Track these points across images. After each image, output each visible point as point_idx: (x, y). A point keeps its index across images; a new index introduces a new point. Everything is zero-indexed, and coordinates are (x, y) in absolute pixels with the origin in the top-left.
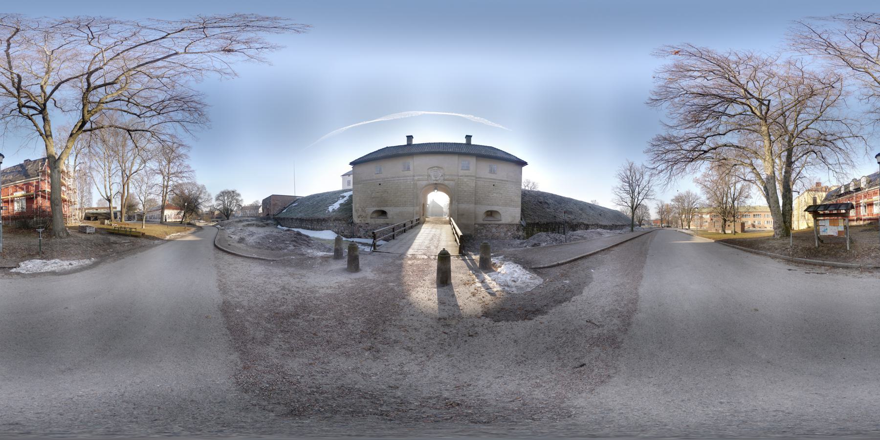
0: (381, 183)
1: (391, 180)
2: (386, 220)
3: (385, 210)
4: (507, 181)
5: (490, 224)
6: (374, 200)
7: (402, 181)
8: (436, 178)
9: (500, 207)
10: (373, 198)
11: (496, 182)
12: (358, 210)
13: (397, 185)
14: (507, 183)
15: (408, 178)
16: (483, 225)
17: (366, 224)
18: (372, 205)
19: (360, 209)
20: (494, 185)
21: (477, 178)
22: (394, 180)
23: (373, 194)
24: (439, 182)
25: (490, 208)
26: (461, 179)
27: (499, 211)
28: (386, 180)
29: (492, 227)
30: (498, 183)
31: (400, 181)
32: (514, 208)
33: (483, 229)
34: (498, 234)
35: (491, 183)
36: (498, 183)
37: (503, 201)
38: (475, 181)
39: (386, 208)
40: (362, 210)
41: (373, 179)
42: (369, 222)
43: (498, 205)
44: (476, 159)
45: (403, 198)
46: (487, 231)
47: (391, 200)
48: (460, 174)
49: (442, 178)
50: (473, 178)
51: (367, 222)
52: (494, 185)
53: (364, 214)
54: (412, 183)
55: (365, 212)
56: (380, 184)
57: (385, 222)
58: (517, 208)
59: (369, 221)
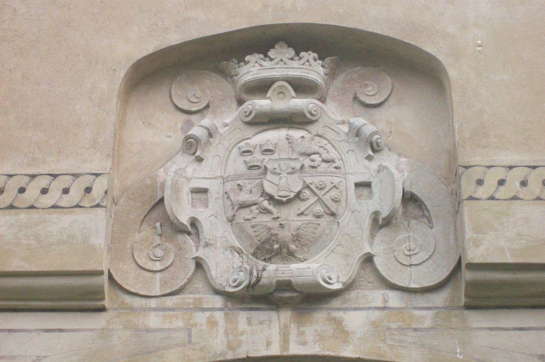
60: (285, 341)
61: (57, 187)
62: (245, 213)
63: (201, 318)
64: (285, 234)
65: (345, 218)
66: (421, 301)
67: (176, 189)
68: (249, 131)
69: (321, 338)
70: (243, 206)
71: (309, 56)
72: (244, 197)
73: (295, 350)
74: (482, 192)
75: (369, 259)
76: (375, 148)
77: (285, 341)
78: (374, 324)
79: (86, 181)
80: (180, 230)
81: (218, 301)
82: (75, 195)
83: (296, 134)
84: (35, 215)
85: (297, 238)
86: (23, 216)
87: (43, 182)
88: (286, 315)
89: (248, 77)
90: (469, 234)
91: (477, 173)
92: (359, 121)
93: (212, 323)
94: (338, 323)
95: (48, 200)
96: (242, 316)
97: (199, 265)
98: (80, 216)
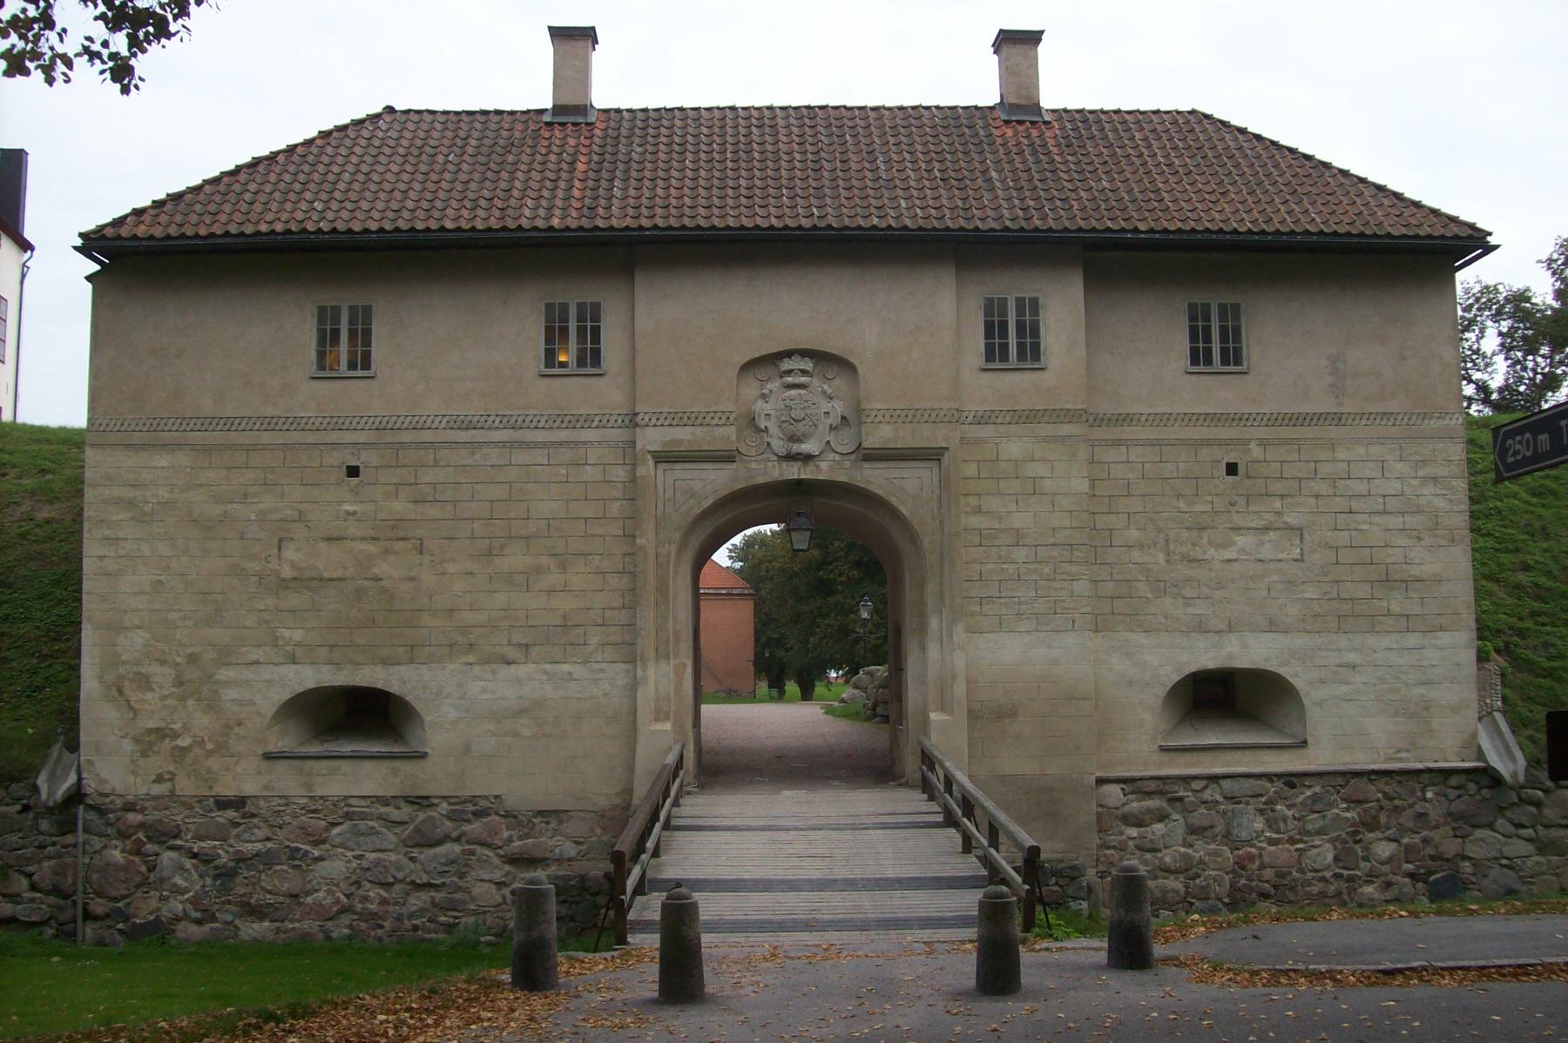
0: (364, 459)
1: (454, 444)
2: (406, 767)
3: (394, 688)
4: (1338, 419)
5: (1214, 779)
6: (293, 600)
7: (540, 456)
8: (794, 439)
9: (1300, 641)
10: (285, 585)
11: (1246, 442)
12: (145, 682)
13: (499, 492)
14: (1334, 432)
15: (589, 435)
16: (1161, 786)
17: (223, 804)
18: (275, 642)
19: (162, 675)
20: (1232, 469)
21: (1098, 421)
22: (473, 446)
23: (290, 553)
24: (823, 471)
25: (1207, 656)
26: (979, 442)
27: (1282, 671)
28: (407, 437)
29: (1230, 799)
30: (1263, 443)
31: (520, 457)
32: (1413, 640)
33: (1162, 817)
34: (1282, 854)
35: (1205, 453)
36: (1263, 443)
37: (1311, 592)
38: (1083, 454)
39: (403, 671)
40: (179, 682)
41: (295, 423)
42: (250, 788)
43: (1273, 626)
44: (1088, 287)
45: (551, 592)
46: (1193, 830)
47: (450, 612)
48: (972, 407)
49: (844, 442)
50: (1065, 430)
51: (227, 789)
52: (1232, 469)
53: (202, 722)
54: (620, 474)
55: (211, 705)
56: (353, 472)
57: (392, 788)
58: (1445, 638)
59: (246, 779)
60: (799, 474)
61: (717, 417)
62: (785, 425)
63: (770, 464)
64: (799, 433)
65: (820, 427)
66: (846, 458)
67: (759, 415)
68: (785, 390)
69: (812, 473)
70: (784, 422)
71: (807, 359)
72: (784, 418)
73: (803, 476)
74: (869, 420)
75: (828, 442)
76: (831, 398)
77: (799, 474)
78: (830, 466)
79: (727, 414)
80: (763, 431)
81: (776, 458)
82: (723, 421)
83: (802, 392)
84: (710, 428)
85: (803, 435)
86: (706, 428)
87: (712, 415)
88: (799, 463)
89: (784, 369)
90: (863, 436)
91: (867, 412)
92: (826, 387)
93: (774, 466)
94: (818, 466)
95: (714, 422)
96: (784, 464)
97: (768, 444)
98: (726, 428)
